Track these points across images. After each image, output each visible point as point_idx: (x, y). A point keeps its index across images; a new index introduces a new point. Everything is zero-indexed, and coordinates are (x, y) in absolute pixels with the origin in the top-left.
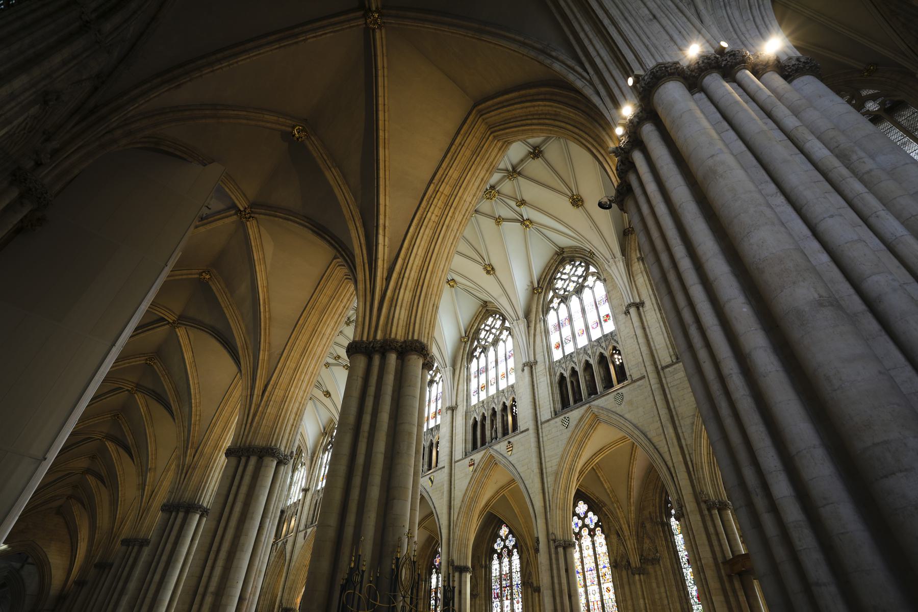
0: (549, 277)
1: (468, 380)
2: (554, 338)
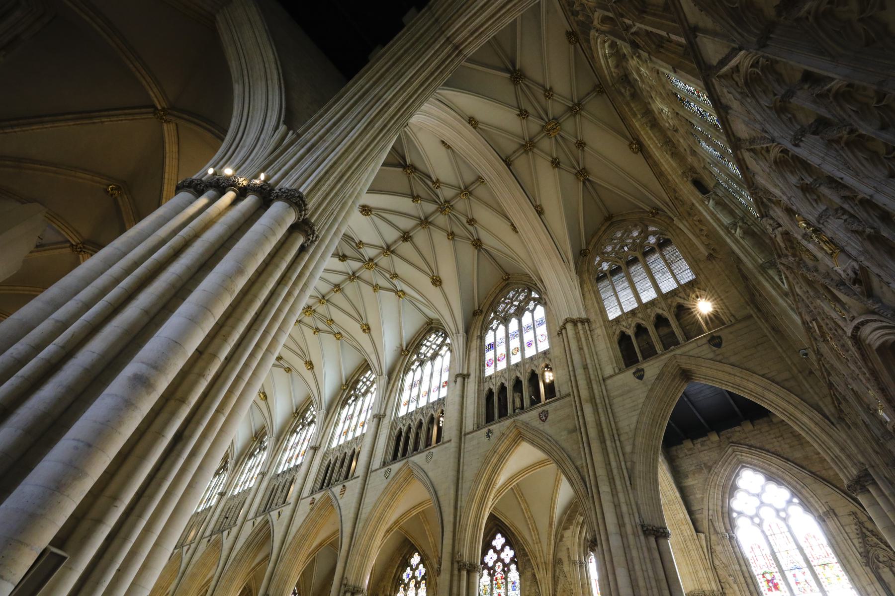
0: (417, 342)
1: (337, 424)
2: (405, 397)
